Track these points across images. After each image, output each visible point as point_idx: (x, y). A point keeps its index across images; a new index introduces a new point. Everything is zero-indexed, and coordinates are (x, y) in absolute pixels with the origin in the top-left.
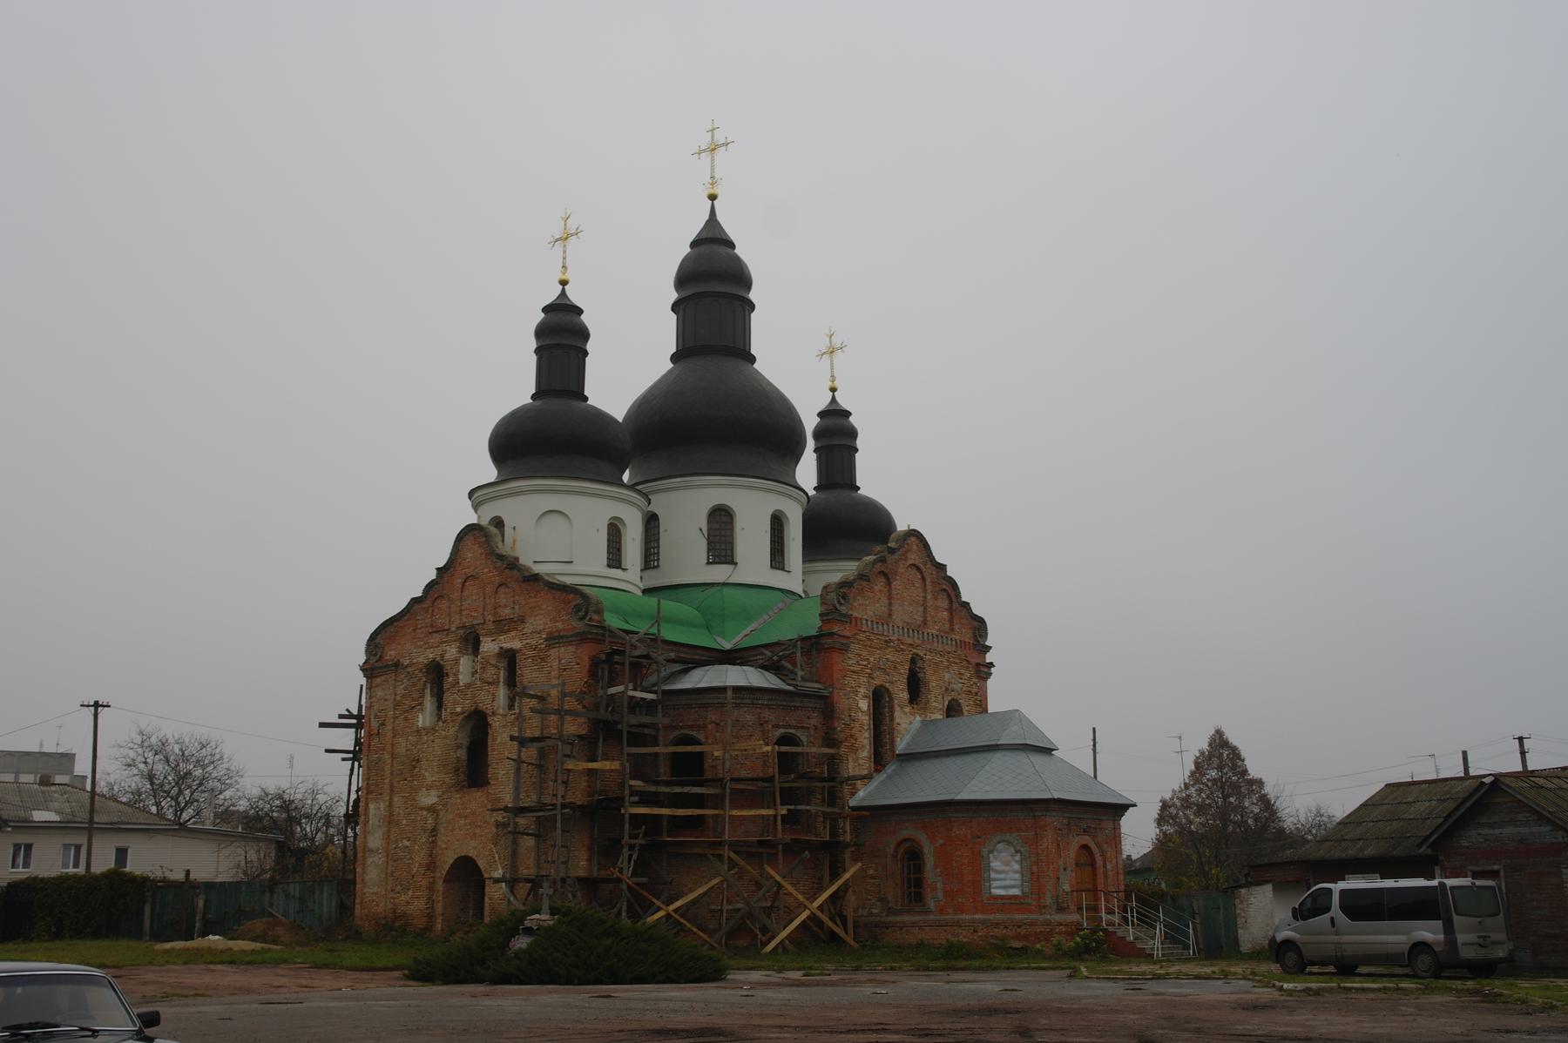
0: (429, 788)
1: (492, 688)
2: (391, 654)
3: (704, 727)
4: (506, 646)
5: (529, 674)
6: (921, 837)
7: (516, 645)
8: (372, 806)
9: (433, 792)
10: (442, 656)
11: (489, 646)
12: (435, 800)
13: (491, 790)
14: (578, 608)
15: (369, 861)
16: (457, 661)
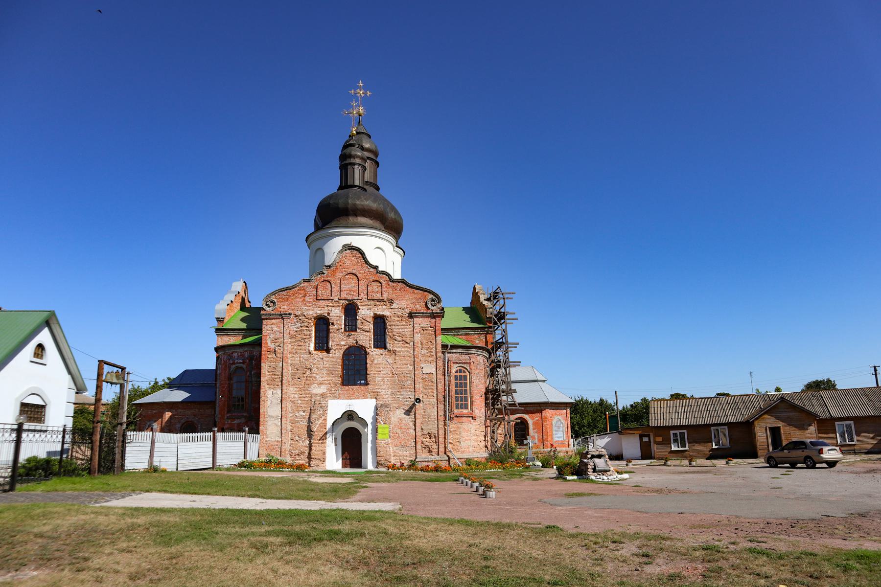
0: (320, 384)
1: (368, 334)
2: (284, 307)
3: (470, 364)
4: (378, 313)
5: (396, 327)
6: (526, 416)
7: (387, 313)
8: (269, 393)
9: (323, 387)
10: (329, 314)
11: (365, 312)
12: (325, 391)
13: (370, 387)
14: (433, 300)
15: (269, 423)
16: (340, 318)
